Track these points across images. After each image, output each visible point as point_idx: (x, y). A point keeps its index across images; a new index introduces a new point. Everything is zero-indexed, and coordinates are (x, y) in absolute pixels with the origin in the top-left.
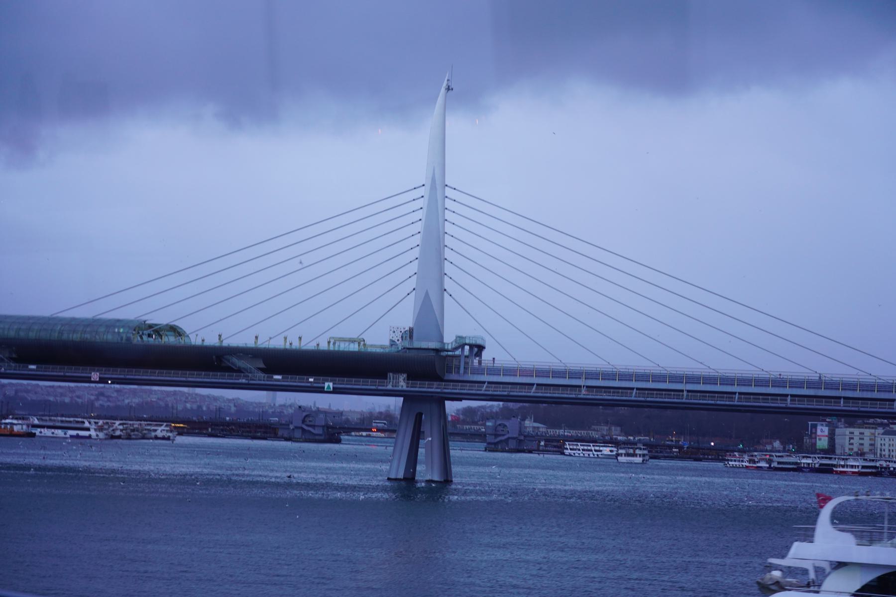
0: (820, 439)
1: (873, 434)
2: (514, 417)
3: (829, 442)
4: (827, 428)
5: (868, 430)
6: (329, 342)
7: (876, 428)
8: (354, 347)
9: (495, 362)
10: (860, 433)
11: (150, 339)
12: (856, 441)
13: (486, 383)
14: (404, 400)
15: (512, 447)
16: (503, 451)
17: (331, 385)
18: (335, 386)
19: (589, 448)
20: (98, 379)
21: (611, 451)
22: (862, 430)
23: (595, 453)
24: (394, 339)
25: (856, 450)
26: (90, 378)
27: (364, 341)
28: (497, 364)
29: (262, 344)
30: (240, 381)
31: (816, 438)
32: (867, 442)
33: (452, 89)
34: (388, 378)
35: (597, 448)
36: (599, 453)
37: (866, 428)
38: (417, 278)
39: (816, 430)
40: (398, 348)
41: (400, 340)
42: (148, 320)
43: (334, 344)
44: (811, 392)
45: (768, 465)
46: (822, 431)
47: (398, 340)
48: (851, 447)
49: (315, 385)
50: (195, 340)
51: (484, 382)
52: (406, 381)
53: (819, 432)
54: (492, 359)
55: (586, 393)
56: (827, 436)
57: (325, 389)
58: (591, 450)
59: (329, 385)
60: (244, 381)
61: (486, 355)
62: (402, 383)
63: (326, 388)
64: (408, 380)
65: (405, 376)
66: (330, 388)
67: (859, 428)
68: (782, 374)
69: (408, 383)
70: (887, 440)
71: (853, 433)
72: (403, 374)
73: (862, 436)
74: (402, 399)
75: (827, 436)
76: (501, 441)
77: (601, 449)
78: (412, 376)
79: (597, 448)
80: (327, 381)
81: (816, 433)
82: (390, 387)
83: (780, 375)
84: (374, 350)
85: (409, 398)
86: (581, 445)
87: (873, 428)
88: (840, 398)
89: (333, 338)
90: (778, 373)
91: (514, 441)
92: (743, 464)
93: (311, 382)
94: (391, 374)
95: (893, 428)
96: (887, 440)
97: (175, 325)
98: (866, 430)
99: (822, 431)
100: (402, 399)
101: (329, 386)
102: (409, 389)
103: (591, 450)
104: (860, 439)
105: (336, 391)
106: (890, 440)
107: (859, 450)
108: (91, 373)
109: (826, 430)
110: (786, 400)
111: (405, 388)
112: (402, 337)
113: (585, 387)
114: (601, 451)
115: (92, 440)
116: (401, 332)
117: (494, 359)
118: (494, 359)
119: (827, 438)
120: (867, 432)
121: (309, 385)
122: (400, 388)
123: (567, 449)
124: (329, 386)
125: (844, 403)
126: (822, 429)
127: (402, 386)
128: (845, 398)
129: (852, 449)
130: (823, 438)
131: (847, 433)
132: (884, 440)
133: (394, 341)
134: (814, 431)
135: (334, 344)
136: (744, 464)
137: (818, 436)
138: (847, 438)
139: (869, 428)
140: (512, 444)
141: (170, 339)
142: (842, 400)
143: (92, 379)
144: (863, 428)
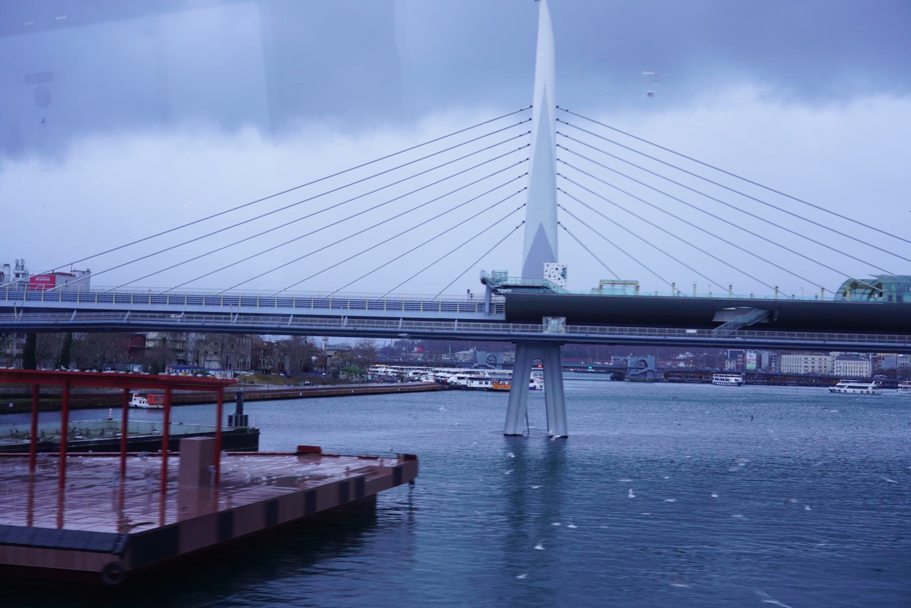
1: (821, 359)
2: (651, 354)
3: (757, 364)
4: (755, 354)
5: (810, 356)
7: (822, 355)
10: (812, 359)
15: (650, 378)
16: (645, 381)
19: (723, 378)
21: (736, 380)
22: (813, 357)
23: (726, 382)
32: (817, 365)
35: (727, 378)
36: (727, 382)
37: (815, 355)
46: (750, 356)
53: (748, 357)
58: (724, 380)
69: (566, 328)
70: (842, 364)
71: (807, 359)
73: (806, 361)
76: (641, 373)
77: (729, 378)
79: (727, 378)
86: (720, 376)
87: (820, 355)
91: (652, 373)
96: (842, 364)
98: (816, 356)
99: (750, 356)
103: (724, 380)
104: (812, 363)
109: (754, 356)
114: (729, 380)
115: (536, 392)
119: (755, 362)
120: (817, 358)
123: (713, 379)
130: (751, 361)
139: (818, 355)
140: (650, 376)
144: (813, 355)
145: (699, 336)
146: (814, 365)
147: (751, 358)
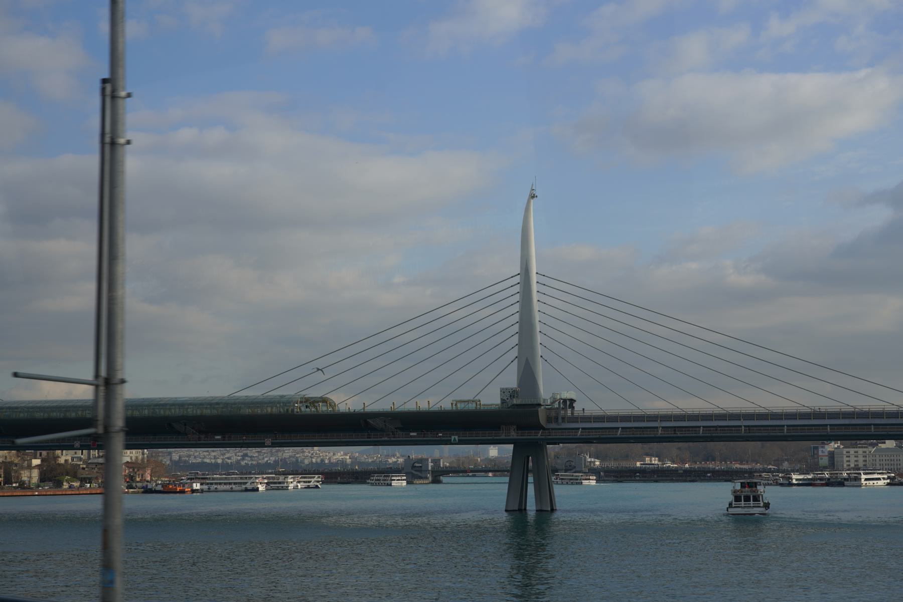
0: (822, 459)
3: (829, 460)
5: (861, 449)
6: (452, 404)
7: (867, 447)
8: (472, 407)
9: (585, 412)
10: (855, 452)
11: (308, 410)
12: (853, 459)
13: (581, 429)
14: (514, 446)
17: (457, 438)
18: (460, 438)
20: (270, 444)
22: (856, 450)
24: (504, 398)
25: (852, 465)
26: (264, 443)
27: (480, 401)
28: (587, 413)
29: (464, 408)
30: (383, 439)
31: (818, 458)
33: (537, 196)
34: (501, 430)
37: (860, 447)
38: (519, 348)
39: (818, 451)
40: (508, 405)
41: (509, 398)
42: (306, 395)
43: (456, 405)
44: (846, 422)
45: (788, 482)
47: (507, 399)
48: (848, 463)
49: (443, 439)
50: (342, 408)
51: (578, 429)
52: (516, 431)
53: (820, 453)
54: (582, 410)
55: (663, 432)
56: (827, 456)
57: (452, 442)
59: (455, 438)
60: (386, 439)
61: (578, 407)
62: (513, 435)
63: (452, 440)
64: (517, 430)
65: (515, 427)
66: (456, 441)
67: (854, 448)
68: (821, 408)
70: (877, 456)
72: (513, 426)
74: (511, 447)
75: (827, 456)
78: (520, 428)
80: (453, 435)
81: (817, 454)
82: (503, 437)
83: (819, 409)
84: (486, 408)
85: (518, 445)
87: (865, 447)
88: (870, 425)
89: (455, 401)
90: (818, 408)
92: (769, 482)
93: (440, 437)
94: (504, 427)
95: (881, 446)
96: (877, 456)
97: (326, 397)
100: (512, 445)
101: (455, 438)
102: (519, 437)
104: (855, 457)
105: (461, 442)
106: (880, 456)
107: (855, 465)
108: (264, 440)
110: (827, 429)
111: (515, 437)
112: (511, 396)
113: (661, 428)
116: (509, 392)
117: (583, 409)
118: (583, 409)
119: (827, 458)
120: (860, 451)
121: (439, 438)
122: (511, 437)
124: (455, 438)
125: (874, 429)
126: (822, 450)
127: (513, 435)
128: (874, 425)
129: (849, 465)
130: (823, 457)
131: (845, 453)
132: (875, 456)
133: (504, 400)
134: (816, 452)
135: (456, 405)
136: (769, 482)
137: (820, 456)
138: (845, 456)
139: (862, 447)
141: (323, 408)
142: (872, 426)
143: (266, 444)
144: (857, 448)
145: (418, 437)
146: (856, 459)
147: (823, 454)
